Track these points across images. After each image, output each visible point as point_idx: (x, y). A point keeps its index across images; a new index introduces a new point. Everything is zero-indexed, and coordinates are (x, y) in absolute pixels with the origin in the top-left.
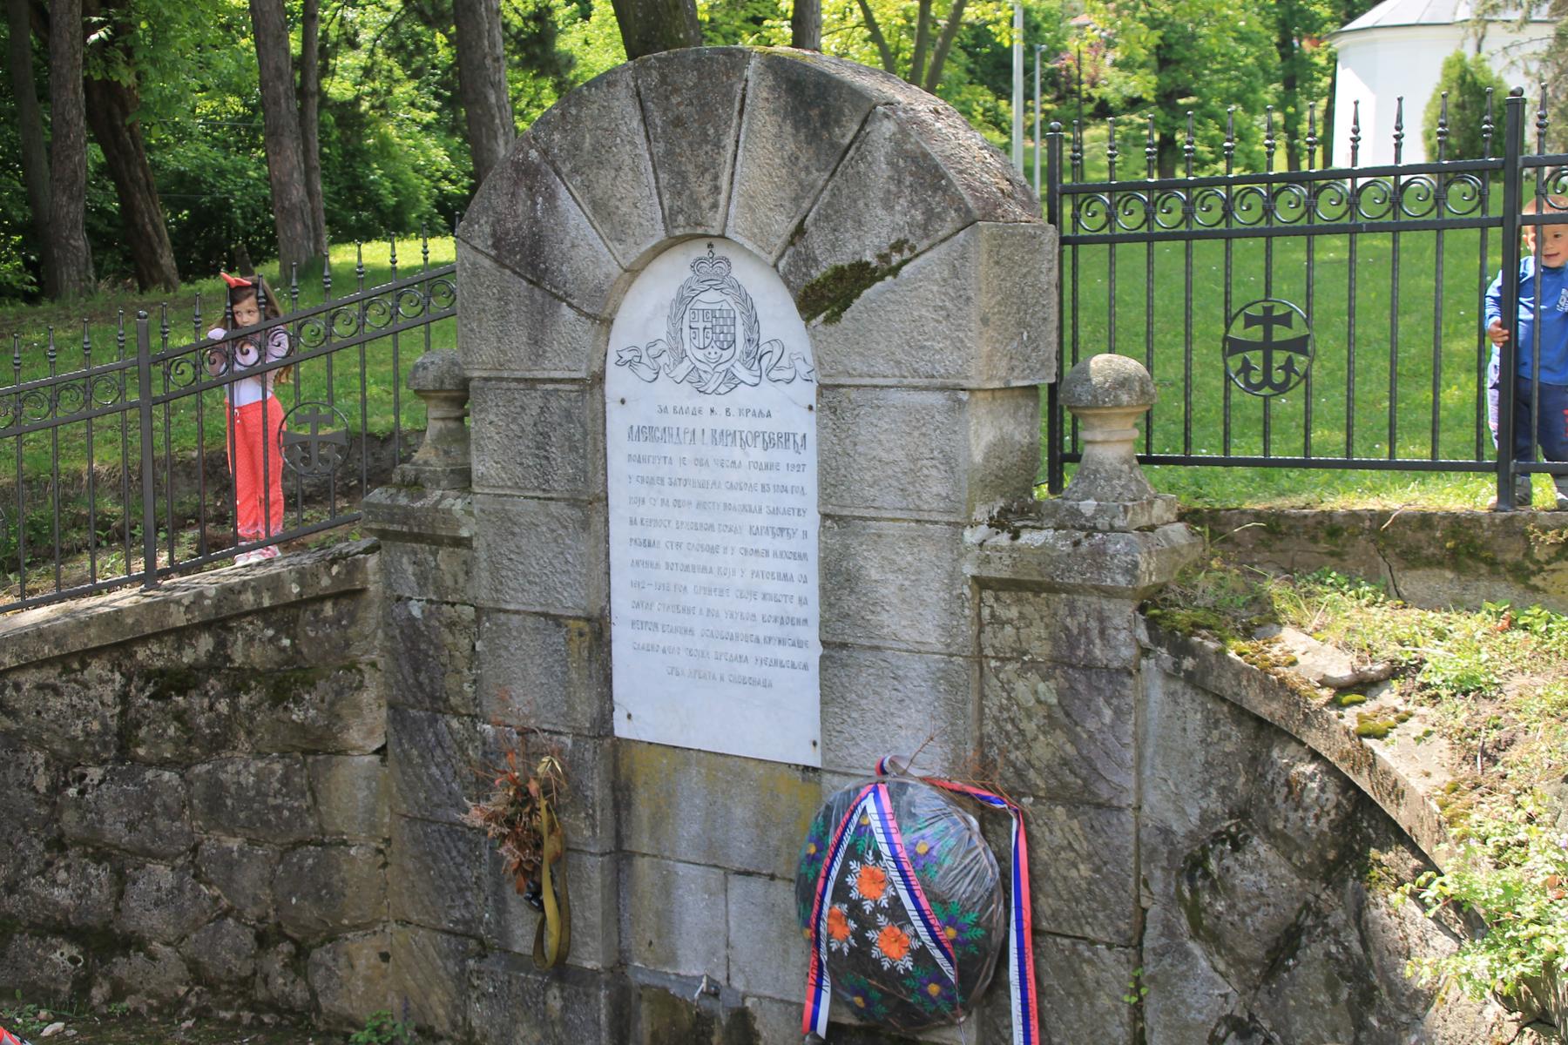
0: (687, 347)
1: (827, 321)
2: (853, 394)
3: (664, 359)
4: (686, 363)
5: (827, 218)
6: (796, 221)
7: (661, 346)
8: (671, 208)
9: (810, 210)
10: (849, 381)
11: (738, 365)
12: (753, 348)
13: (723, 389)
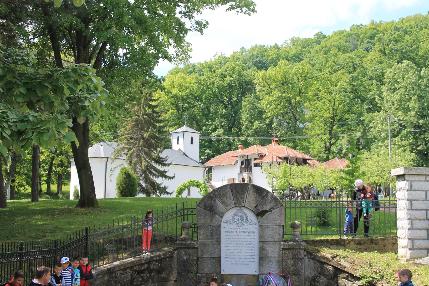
4: (235, 223)
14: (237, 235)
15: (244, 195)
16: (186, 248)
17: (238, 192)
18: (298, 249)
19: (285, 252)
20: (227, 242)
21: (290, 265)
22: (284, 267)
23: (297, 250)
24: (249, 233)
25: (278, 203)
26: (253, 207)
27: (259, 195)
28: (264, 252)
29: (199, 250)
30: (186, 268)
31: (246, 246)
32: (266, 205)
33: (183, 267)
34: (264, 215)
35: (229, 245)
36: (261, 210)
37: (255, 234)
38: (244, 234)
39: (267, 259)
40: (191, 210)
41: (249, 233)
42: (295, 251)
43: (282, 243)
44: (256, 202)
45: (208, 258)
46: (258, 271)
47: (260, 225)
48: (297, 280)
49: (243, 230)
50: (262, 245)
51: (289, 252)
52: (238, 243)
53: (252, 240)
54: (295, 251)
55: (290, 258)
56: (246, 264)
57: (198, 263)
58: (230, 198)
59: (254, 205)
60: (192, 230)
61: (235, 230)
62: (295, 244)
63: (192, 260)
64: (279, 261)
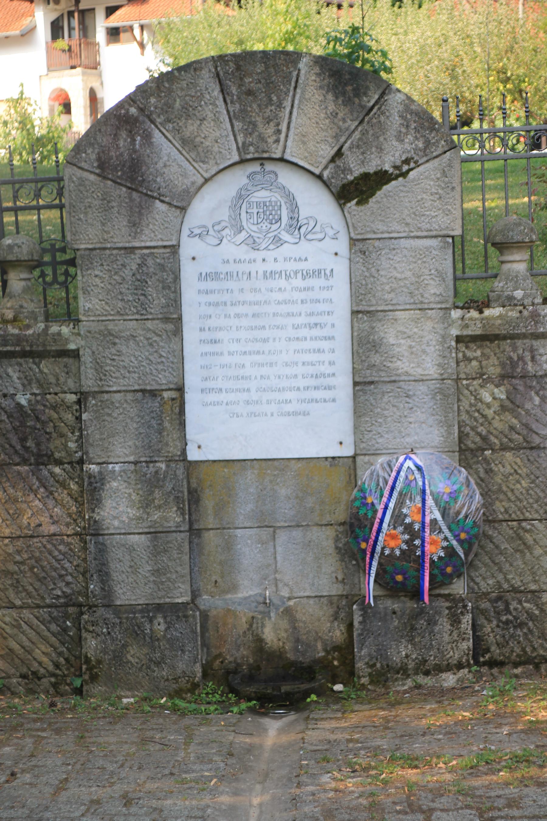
0: (244, 223)
1: (358, 204)
2: (377, 243)
3: (227, 231)
4: (244, 233)
5: (358, 147)
6: (336, 149)
7: (223, 224)
8: (244, 143)
9: (345, 142)
10: (374, 236)
11: (283, 233)
12: (294, 222)
13: (272, 247)
14: (254, 290)
15: (280, 106)
16: (25, 354)
17: (250, 93)
18: (524, 336)
19: (469, 354)
20: (212, 323)
21: (489, 406)
22: (464, 417)
23: (519, 343)
24: (306, 275)
25: (432, 136)
26: (324, 162)
27: (348, 102)
28: (376, 359)
29: (86, 357)
30: (30, 443)
31: (293, 333)
32: (380, 149)
33: (14, 440)
34: (372, 195)
35: (220, 335)
36: (357, 171)
37: (331, 282)
38: (282, 283)
39: (389, 387)
40: (33, 185)
41: (306, 275)
42: (515, 349)
43: (456, 314)
44: (336, 137)
45: (130, 396)
46: (349, 440)
47: (353, 242)
48: (524, 471)
49: (278, 267)
50: (366, 326)
51: (487, 351)
52: (259, 322)
53: (321, 307)
54: (515, 349)
55: (489, 380)
56: (296, 414)
57: (84, 416)
58: (216, 120)
59: (329, 151)
60: (43, 275)
61: (241, 268)
62: (514, 314)
63: (54, 408)
64: (441, 391)
